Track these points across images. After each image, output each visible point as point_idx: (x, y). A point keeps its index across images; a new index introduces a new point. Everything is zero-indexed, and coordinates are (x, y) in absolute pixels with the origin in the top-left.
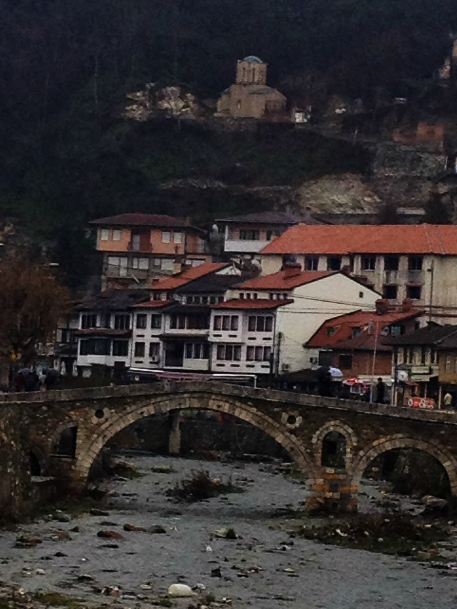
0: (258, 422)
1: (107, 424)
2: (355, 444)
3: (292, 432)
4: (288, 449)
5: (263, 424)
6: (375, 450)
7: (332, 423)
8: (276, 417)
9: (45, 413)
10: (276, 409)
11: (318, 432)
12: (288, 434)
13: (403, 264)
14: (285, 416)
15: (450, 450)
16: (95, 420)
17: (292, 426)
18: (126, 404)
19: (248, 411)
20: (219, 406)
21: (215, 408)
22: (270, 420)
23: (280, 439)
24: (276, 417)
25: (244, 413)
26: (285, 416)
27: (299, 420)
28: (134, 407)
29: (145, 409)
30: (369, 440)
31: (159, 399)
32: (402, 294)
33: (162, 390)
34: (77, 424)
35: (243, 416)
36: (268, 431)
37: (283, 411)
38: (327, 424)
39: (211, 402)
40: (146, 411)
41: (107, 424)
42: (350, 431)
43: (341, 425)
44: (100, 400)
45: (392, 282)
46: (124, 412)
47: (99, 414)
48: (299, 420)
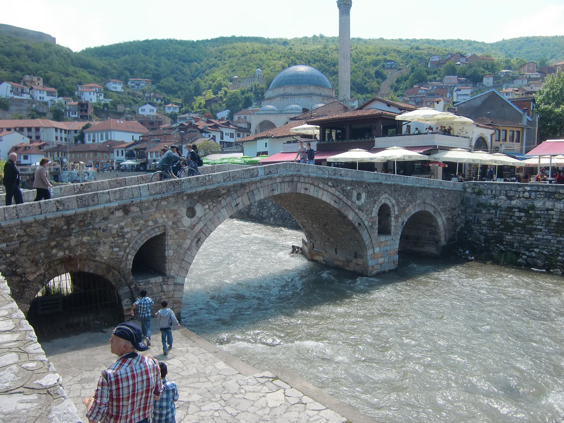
0: (335, 202)
1: (201, 225)
2: (396, 213)
3: (360, 208)
4: (357, 225)
5: (339, 203)
6: (406, 216)
7: (384, 196)
8: (348, 195)
9: (121, 221)
10: (349, 188)
11: (376, 206)
12: (357, 211)
13: (33, 130)
14: (355, 194)
15: (441, 209)
16: (187, 221)
17: (358, 203)
18: (219, 196)
19: (328, 191)
20: (306, 189)
21: (303, 192)
22: (345, 199)
23: (351, 216)
24: (348, 195)
25: (325, 193)
26: (355, 194)
27: (364, 195)
28: (229, 199)
29: (239, 200)
30: (404, 208)
31: (253, 187)
32: (34, 138)
33: (256, 176)
34: (165, 229)
35: (326, 198)
36: (342, 211)
37: (353, 189)
38: (381, 198)
39: (299, 185)
40: (241, 203)
41: (201, 225)
42: (394, 202)
43: (388, 197)
44: (190, 196)
45: (30, 135)
46: (219, 206)
47: (191, 213)
48: (364, 195)
